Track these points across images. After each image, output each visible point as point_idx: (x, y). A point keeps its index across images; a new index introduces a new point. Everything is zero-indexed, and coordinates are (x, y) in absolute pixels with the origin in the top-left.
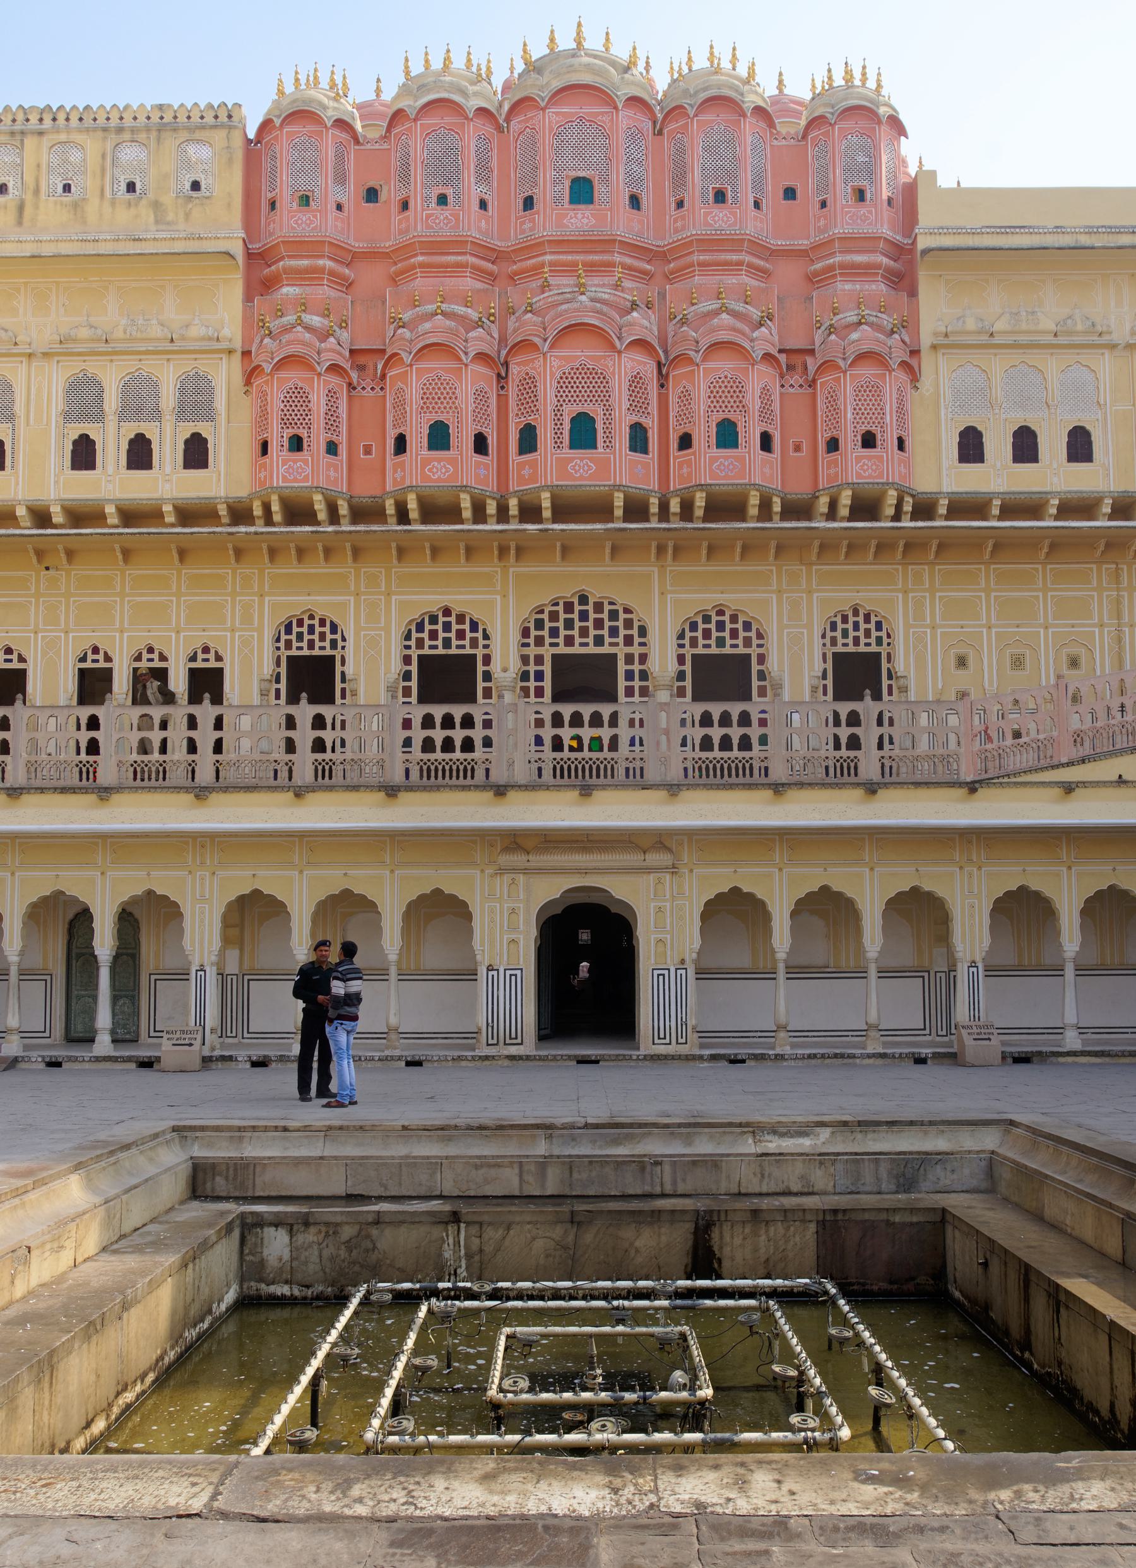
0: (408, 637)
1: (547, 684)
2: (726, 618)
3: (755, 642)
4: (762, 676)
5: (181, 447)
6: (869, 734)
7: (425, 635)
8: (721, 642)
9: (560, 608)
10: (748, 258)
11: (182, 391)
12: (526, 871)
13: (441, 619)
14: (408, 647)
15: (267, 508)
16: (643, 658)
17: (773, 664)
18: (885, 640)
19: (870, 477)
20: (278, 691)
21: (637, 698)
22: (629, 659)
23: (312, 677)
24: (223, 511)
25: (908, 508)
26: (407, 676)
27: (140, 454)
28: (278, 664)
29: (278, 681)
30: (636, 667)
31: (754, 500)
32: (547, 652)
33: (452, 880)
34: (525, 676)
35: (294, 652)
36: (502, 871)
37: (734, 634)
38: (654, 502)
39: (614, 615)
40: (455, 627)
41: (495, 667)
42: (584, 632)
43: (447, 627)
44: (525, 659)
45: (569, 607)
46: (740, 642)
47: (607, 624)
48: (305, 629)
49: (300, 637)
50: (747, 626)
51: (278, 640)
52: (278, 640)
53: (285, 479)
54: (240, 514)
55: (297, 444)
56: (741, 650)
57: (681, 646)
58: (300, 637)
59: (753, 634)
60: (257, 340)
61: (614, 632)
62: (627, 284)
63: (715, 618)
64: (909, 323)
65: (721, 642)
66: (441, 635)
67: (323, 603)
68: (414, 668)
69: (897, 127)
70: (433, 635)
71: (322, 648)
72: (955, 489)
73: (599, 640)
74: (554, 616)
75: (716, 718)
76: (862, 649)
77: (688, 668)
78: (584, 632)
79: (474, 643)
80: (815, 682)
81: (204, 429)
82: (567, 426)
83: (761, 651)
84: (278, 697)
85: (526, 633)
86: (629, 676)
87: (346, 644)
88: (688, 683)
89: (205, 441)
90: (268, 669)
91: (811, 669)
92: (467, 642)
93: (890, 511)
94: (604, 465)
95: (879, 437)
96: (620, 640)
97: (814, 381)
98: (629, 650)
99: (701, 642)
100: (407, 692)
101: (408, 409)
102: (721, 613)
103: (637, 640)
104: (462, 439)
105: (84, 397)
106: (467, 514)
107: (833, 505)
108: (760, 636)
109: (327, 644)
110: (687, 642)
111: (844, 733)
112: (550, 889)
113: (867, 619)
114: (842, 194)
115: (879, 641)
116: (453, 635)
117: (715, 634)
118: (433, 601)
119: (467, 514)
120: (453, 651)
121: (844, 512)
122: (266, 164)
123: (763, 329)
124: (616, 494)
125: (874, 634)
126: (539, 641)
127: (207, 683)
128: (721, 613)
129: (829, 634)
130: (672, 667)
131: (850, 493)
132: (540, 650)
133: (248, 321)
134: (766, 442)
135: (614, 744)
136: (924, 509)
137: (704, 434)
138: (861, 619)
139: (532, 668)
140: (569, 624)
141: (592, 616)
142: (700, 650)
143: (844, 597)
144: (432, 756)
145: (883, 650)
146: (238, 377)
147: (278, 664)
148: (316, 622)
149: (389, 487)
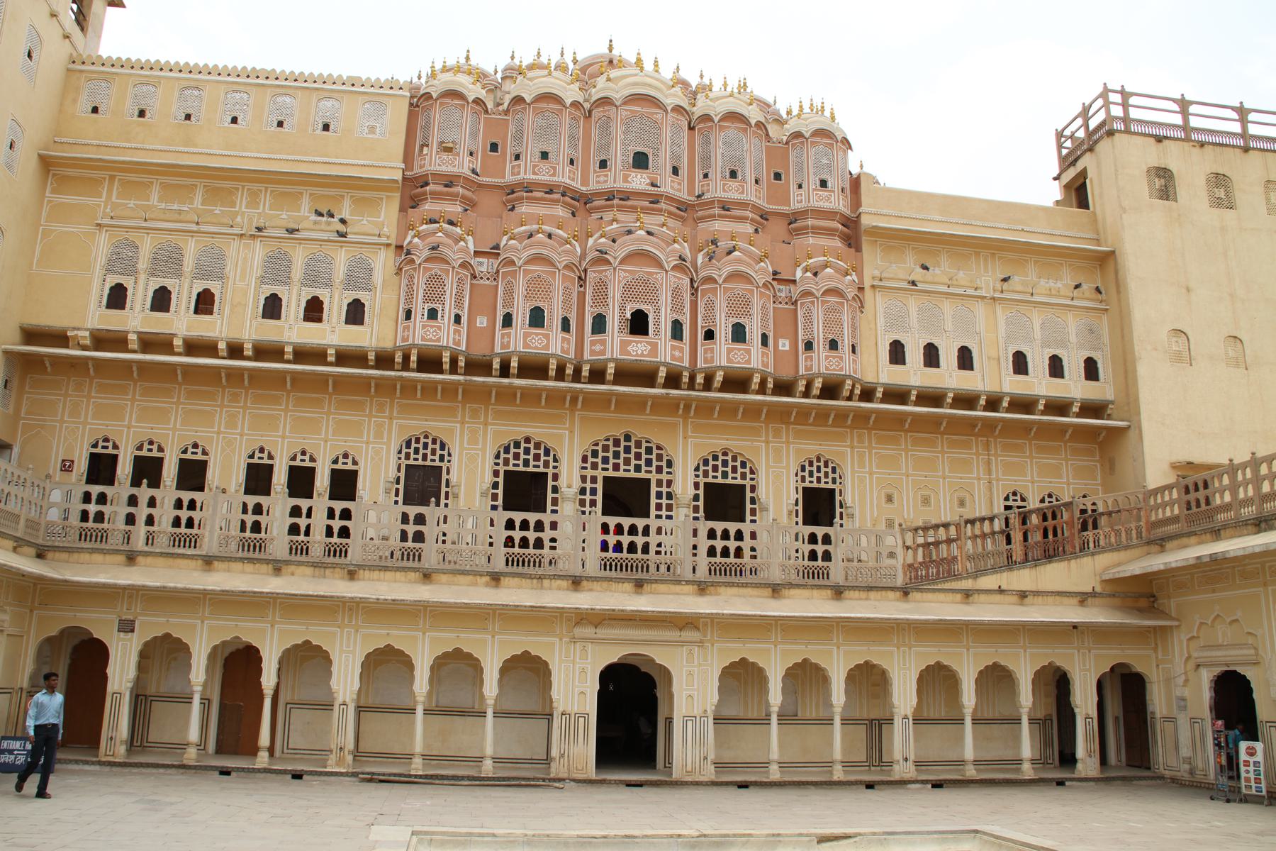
0: (497, 457)
1: (599, 498)
2: (729, 458)
3: (749, 476)
4: (753, 501)
5: (345, 308)
6: (838, 552)
7: (511, 456)
8: (725, 475)
9: (611, 443)
10: (751, 215)
12: (593, 640)
13: (523, 445)
14: (497, 464)
15: (406, 358)
16: (669, 483)
17: (762, 493)
18: (838, 480)
20: (397, 490)
21: (664, 513)
22: (659, 483)
23: (423, 484)
24: (371, 356)
25: (857, 392)
26: (495, 485)
27: (314, 310)
28: (399, 470)
29: (398, 483)
30: (664, 490)
31: (756, 379)
32: (600, 474)
33: (536, 644)
34: (583, 491)
35: (411, 462)
36: (574, 640)
37: (734, 469)
38: (686, 374)
39: (649, 451)
40: (533, 451)
41: (562, 483)
42: (627, 462)
43: (527, 451)
44: (583, 479)
45: (617, 443)
46: (738, 475)
47: (644, 456)
48: (421, 446)
49: (417, 451)
50: (744, 465)
51: (400, 452)
52: (400, 452)
54: (384, 360)
55: (433, 314)
56: (739, 481)
57: (697, 476)
58: (417, 451)
59: (747, 470)
60: (408, 239)
61: (649, 463)
62: (671, 223)
63: (721, 457)
64: (857, 269)
65: (725, 475)
66: (523, 457)
67: (435, 425)
68: (501, 480)
69: (846, 143)
70: (517, 456)
71: (433, 460)
73: (638, 469)
74: (606, 449)
75: (732, 534)
76: (822, 485)
77: (701, 492)
78: (627, 462)
79: (546, 464)
80: (791, 507)
81: (363, 297)
82: (629, 316)
83: (753, 483)
84: (397, 495)
85: (585, 459)
86: (659, 495)
87: (452, 459)
88: (701, 503)
90: (392, 474)
91: (788, 498)
92: (541, 463)
93: (846, 393)
94: (654, 346)
96: (653, 469)
98: (659, 476)
99: (711, 474)
100: (495, 497)
102: (725, 454)
103: (665, 469)
104: (553, 318)
105: (277, 267)
106: (552, 373)
107: (809, 386)
108: (752, 472)
109: (437, 457)
110: (700, 473)
111: (820, 548)
112: (613, 655)
113: (826, 465)
114: (814, 182)
115: (834, 481)
116: (531, 457)
117: (721, 469)
118: (518, 430)
119: (552, 373)
120: (531, 469)
121: (816, 391)
122: (421, 121)
124: (662, 368)
125: (831, 475)
126: (594, 466)
127: (344, 484)
128: (725, 454)
129: (800, 474)
130: (691, 492)
131: (821, 380)
132: (594, 473)
134: (765, 339)
135: (646, 549)
136: (867, 395)
137: (723, 331)
138: (822, 464)
139: (588, 485)
140: (616, 455)
141: (633, 450)
142: (710, 480)
143: (812, 448)
144: (526, 551)
145: (837, 487)
147: (399, 470)
148: (430, 441)
149: (498, 350)
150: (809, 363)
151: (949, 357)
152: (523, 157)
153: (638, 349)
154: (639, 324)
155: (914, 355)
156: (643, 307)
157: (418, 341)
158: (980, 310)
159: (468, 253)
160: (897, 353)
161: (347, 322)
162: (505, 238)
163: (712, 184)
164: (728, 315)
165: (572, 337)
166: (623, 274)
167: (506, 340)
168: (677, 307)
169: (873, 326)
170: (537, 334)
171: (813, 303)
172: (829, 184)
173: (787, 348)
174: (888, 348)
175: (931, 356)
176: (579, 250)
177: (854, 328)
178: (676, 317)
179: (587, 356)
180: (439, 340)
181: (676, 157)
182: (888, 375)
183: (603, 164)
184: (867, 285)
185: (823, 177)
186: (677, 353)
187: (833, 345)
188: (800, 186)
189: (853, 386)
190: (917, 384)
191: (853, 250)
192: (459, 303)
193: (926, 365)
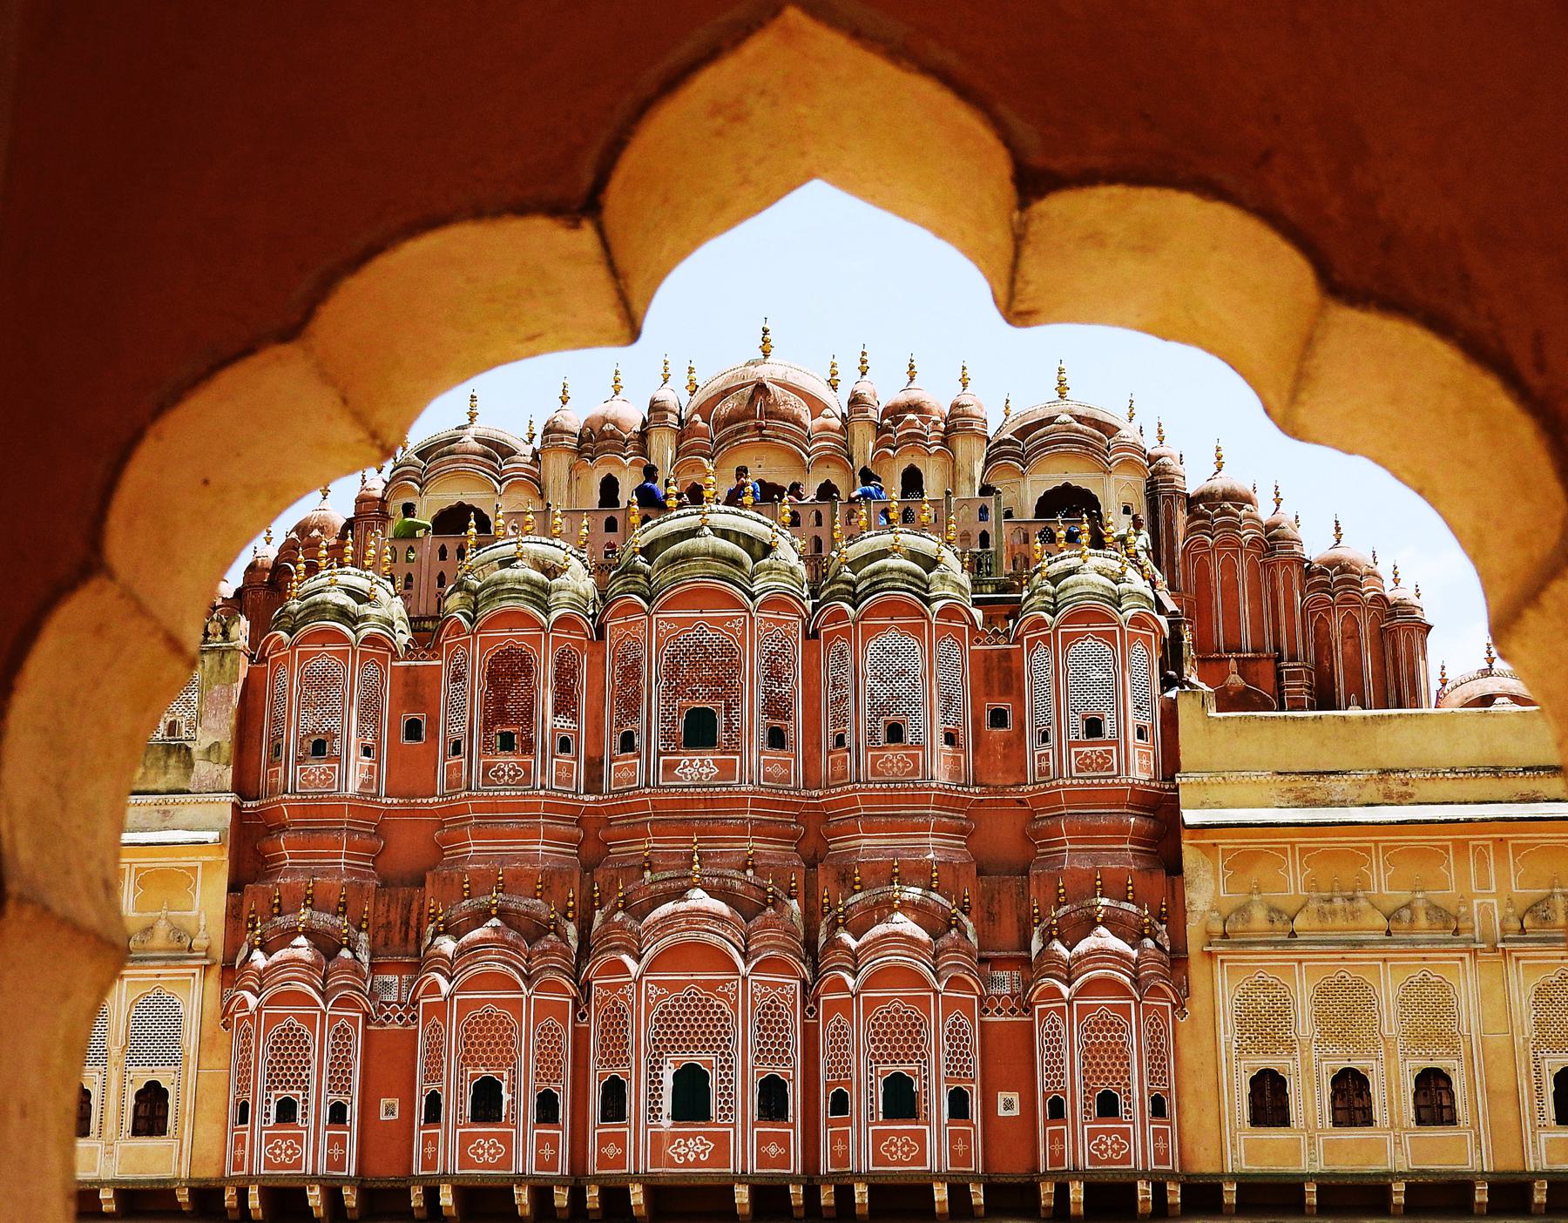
5: (131, 1101)
11: (138, 1020)
19: (1110, 1161)
24: (183, 1197)
53: (269, 1164)
55: (286, 1111)
64: (1173, 913)
72: (1245, 1167)
89: (165, 1093)
94: (721, 1141)
95: (1121, 1100)
97: (1032, 1005)
101: (445, 1059)
104: (517, 1099)
123: (953, 932)
133: (234, 914)
134: (959, 1105)
137: (868, 1096)
146: (213, 1005)
149: (417, 1170)
150: (1057, 1147)
151: (1392, 1094)
152: (464, 747)
153: (689, 1153)
154: (692, 1098)
155: (1309, 1099)
156: (698, 1058)
157: (260, 1169)
158: (1468, 985)
159: (357, 972)
160: (1269, 1098)
161: (136, 1132)
162: (430, 929)
163: (850, 759)
164: (876, 1059)
165: (563, 1135)
166: (654, 991)
167: (430, 1150)
168: (772, 1047)
169: (1207, 1043)
170: (487, 1136)
171: (1060, 1011)
172: (1107, 728)
173: (1016, 1112)
174: (1247, 1089)
175: (1351, 1097)
176: (574, 944)
177: (1157, 1059)
178: (768, 1069)
179: (593, 1168)
180: (297, 1164)
181: (776, 707)
182: (1245, 1150)
183: (627, 742)
184: (1194, 945)
185: (1093, 712)
186: (773, 1150)
187: (1108, 1106)
188: (1045, 738)
189: (1159, 1191)
190: (1319, 1167)
191: (1161, 877)
192: (339, 1081)
193: (1336, 1123)
